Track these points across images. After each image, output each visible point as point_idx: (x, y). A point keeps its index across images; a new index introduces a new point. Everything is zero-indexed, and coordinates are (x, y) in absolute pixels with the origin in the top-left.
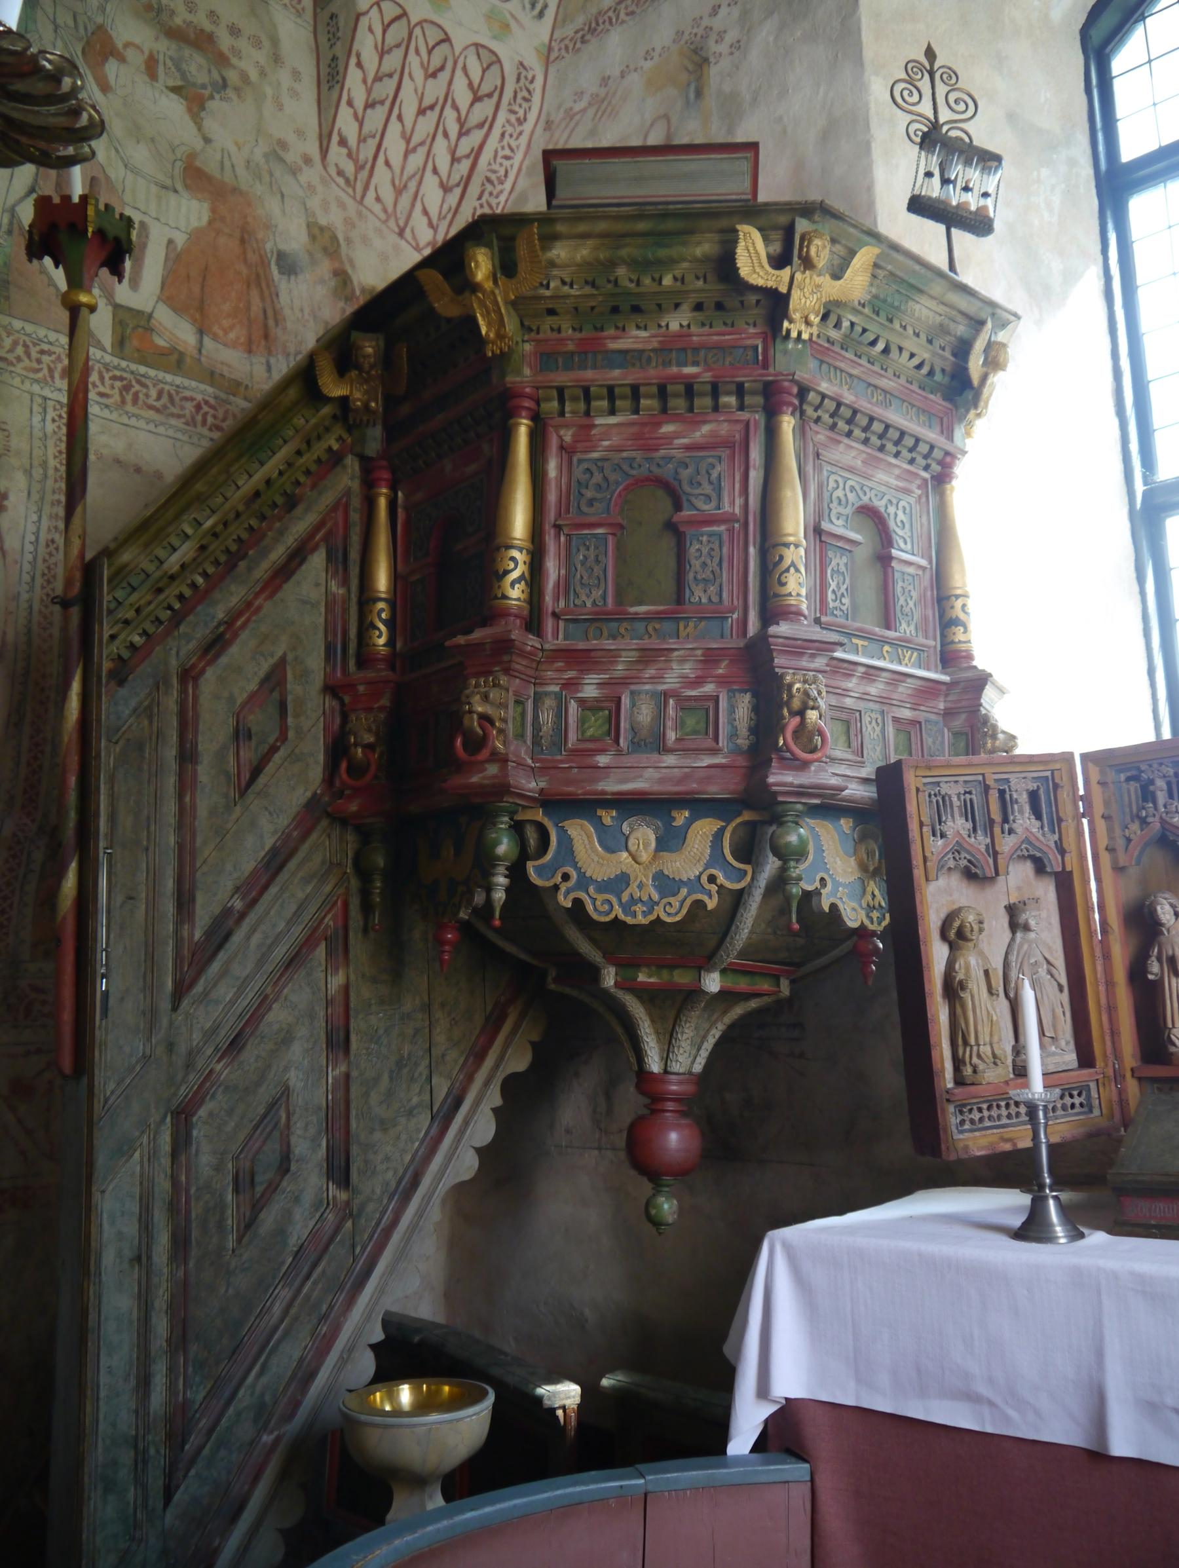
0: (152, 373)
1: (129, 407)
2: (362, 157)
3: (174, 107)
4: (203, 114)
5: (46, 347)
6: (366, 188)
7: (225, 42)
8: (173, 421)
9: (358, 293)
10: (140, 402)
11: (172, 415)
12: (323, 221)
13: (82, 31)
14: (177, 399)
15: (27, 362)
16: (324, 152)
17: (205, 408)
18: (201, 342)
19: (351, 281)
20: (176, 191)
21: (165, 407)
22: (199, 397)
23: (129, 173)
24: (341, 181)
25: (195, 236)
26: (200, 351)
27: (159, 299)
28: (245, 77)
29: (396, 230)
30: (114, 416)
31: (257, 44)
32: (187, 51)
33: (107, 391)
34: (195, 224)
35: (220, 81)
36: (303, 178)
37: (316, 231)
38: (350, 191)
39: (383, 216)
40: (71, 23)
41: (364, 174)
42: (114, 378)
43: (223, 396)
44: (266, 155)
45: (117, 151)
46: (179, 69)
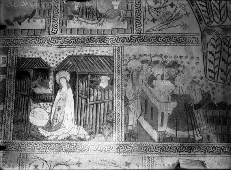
0: (166, 143)
1: (162, 153)
2: (215, 71)
3: (169, 83)
4: (175, 81)
5: (145, 146)
6: (218, 78)
7: (179, 60)
8: (171, 153)
9: (216, 106)
10: (164, 151)
11: (171, 152)
12: (206, 92)
13: (147, 78)
14: (172, 147)
15: (142, 150)
16: (206, 74)
17: (178, 148)
18: (177, 133)
19: (214, 104)
20: (169, 102)
21: (169, 150)
22: (176, 146)
23: (159, 103)
24: (211, 79)
25: (174, 110)
26: (176, 135)
27: (167, 126)
28: (184, 67)
29: (228, 84)
30: (159, 155)
31: (187, 57)
32: (170, 69)
33: (157, 150)
34: (174, 107)
35: (178, 72)
36: (200, 84)
37: (204, 95)
38: (214, 80)
39: (223, 82)
40: (145, 78)
41: (216, 75)
42: (159, 147)
43: (182, 143)
44: (190, 83)
45: (156, 99)
46: (168, 74)
